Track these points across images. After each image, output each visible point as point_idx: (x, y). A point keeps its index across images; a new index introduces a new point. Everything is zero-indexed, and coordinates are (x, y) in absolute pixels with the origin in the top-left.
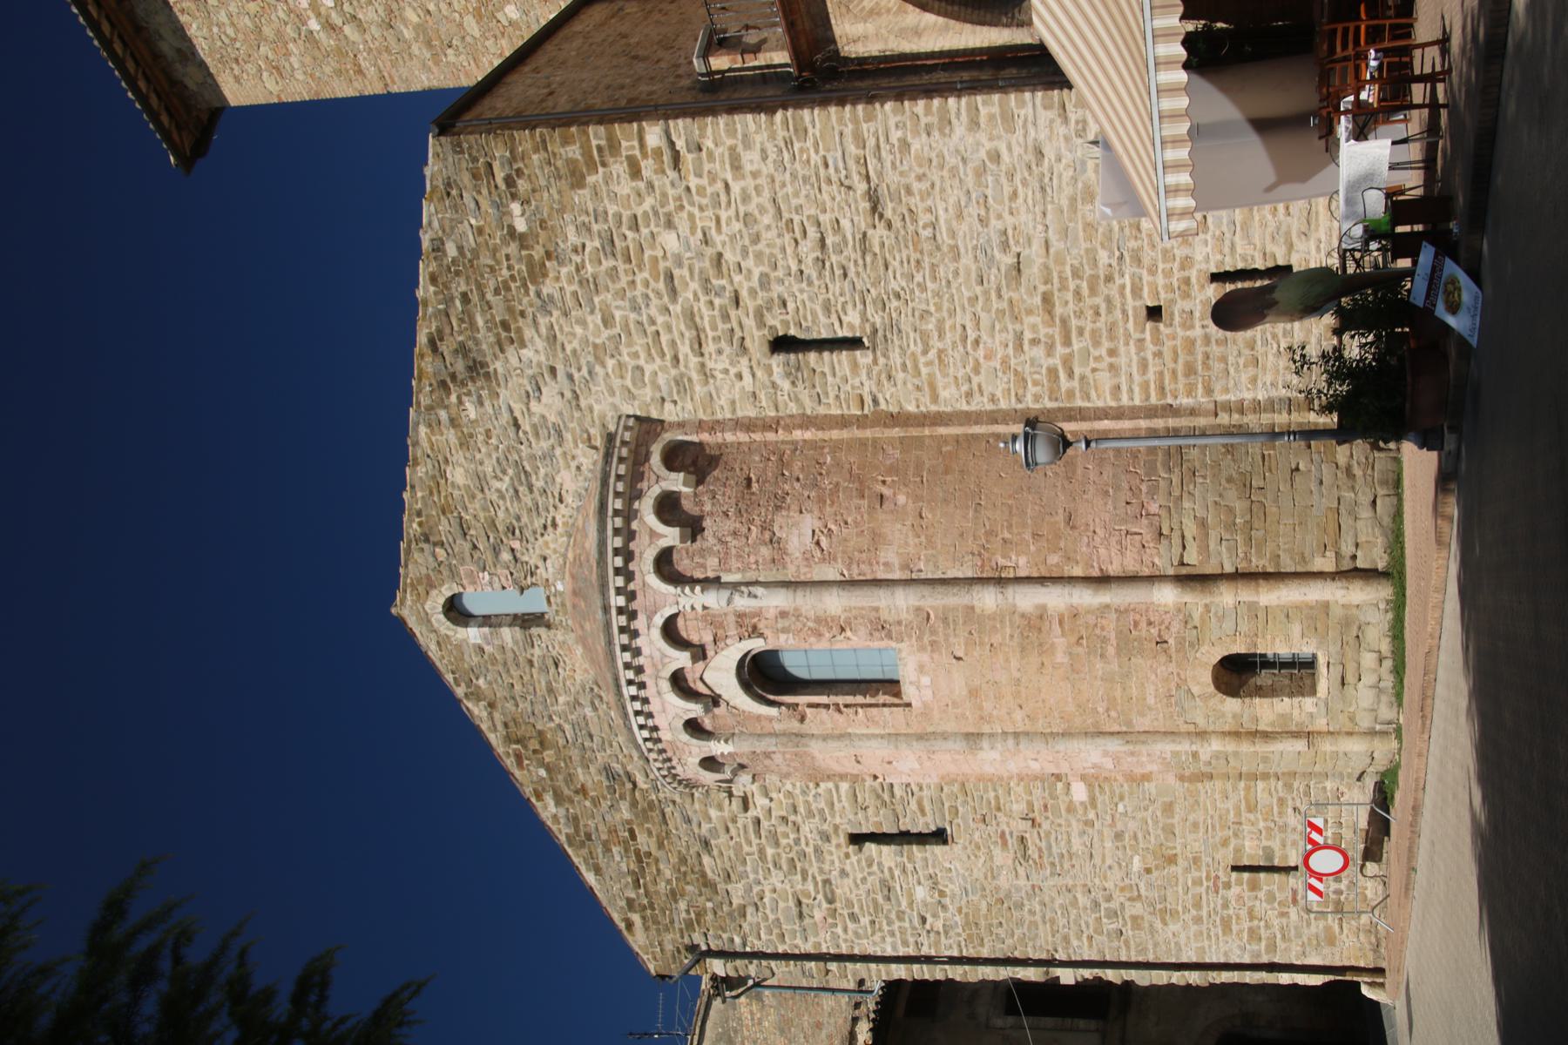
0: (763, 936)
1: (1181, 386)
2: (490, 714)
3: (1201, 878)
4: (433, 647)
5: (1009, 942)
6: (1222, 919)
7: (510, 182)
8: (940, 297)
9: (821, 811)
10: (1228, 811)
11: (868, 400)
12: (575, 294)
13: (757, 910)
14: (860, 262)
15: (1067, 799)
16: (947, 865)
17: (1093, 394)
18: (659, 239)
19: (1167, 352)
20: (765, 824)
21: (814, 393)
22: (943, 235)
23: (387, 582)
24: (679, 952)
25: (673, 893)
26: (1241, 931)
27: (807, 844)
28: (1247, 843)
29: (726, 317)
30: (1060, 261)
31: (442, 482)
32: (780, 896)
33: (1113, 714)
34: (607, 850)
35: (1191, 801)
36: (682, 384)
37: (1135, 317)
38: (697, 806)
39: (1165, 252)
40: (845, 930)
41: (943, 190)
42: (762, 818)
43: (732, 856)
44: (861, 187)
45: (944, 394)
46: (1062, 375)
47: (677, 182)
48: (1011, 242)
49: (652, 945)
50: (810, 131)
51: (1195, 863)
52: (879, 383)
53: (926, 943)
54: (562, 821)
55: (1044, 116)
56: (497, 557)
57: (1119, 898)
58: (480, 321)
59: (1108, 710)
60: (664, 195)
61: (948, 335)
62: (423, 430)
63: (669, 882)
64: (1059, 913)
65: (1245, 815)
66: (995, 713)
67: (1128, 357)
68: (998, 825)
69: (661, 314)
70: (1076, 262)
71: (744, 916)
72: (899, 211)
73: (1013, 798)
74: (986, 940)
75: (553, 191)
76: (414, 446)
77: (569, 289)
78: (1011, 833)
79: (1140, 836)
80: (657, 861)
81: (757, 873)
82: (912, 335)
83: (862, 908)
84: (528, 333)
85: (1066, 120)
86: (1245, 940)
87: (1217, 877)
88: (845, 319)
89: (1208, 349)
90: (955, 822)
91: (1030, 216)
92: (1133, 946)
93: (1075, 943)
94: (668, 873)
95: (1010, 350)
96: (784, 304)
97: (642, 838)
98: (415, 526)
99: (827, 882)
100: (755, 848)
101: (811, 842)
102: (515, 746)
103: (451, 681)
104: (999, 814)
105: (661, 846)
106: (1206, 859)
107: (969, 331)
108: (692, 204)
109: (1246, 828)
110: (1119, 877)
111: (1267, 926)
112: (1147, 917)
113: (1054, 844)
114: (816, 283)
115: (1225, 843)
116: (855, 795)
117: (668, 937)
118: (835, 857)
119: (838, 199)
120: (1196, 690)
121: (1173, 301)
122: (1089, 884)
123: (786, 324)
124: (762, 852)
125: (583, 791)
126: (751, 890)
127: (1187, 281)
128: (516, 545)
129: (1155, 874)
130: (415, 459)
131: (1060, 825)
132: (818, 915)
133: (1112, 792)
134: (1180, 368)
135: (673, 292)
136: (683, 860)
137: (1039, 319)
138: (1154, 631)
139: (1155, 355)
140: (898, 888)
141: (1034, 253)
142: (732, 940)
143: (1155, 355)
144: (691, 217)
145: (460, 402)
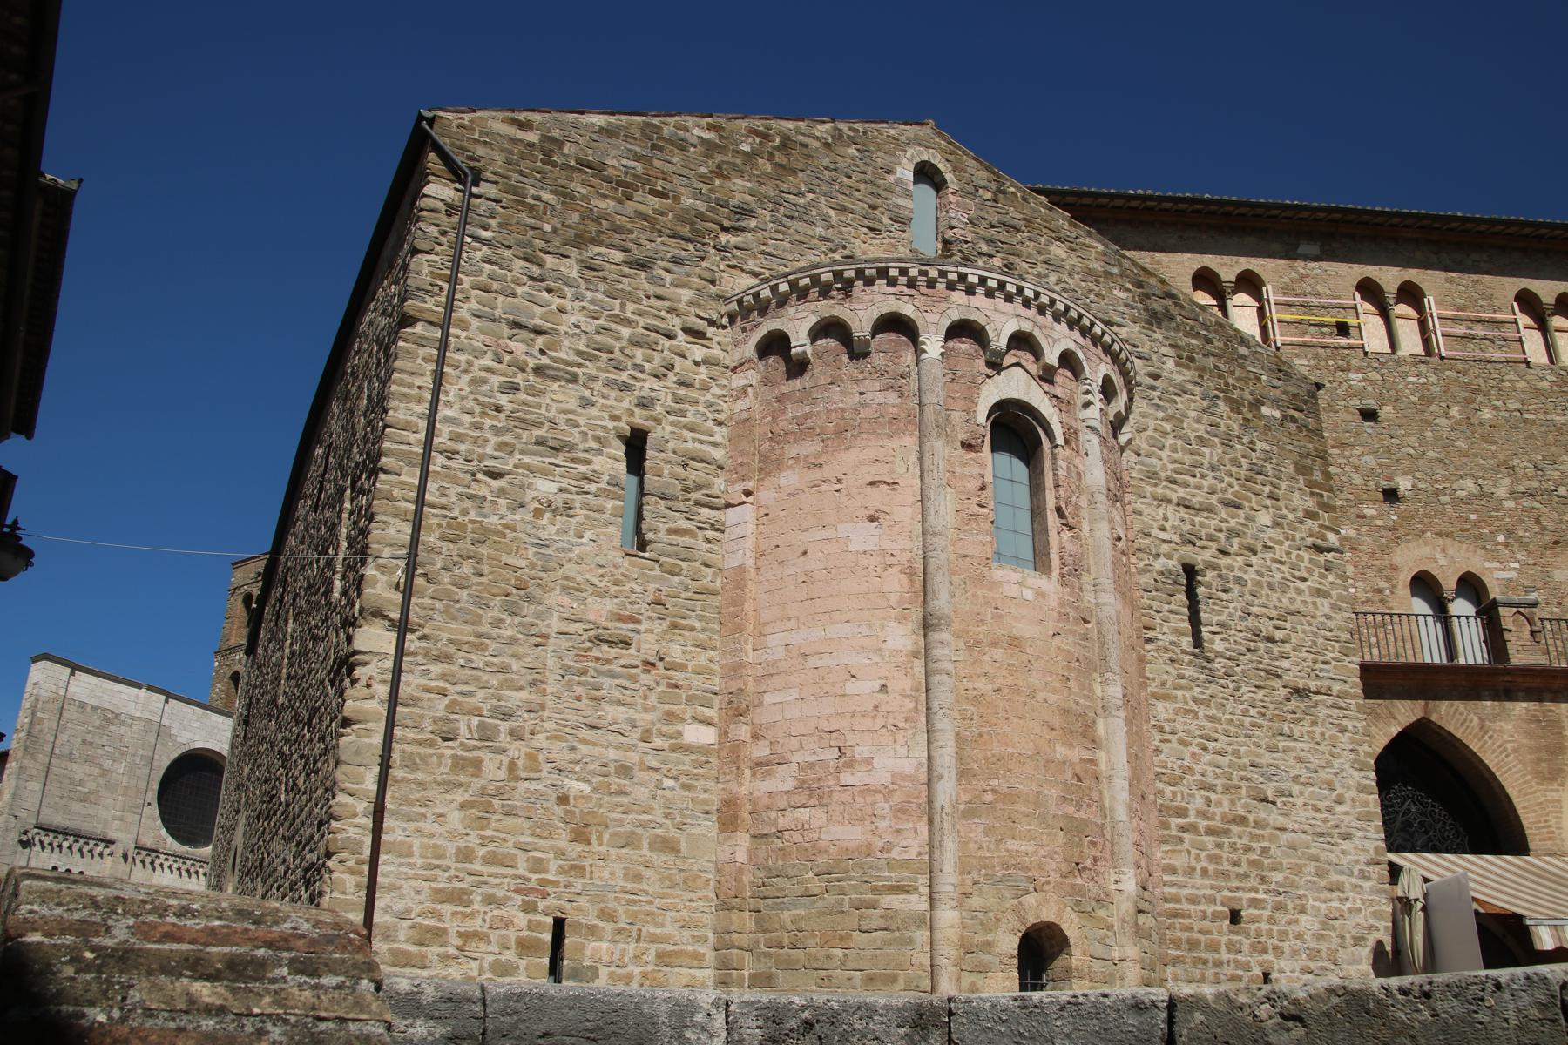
0: (487, 266)
1: (1178, 934)
2: (817, 138)
3: (546, 872)
4: (892, 132)
5: (446, 578)
6: (463, 891)
7: (1293, 420)
8: (1238, 726)
9: (682, 414)
10: (661, 926)
11: (1150, 634)
12: (1218, 425)
13: (532, 278)
14: (1261, 666)
15: (687, 716)
16: (588, 535)
17: (1166, 847)
18: (1264, 510)
19: (1207, 924)
20: (667, 343)
21: (1152, 588)
22: (1282, 743)
23: (960, 131)
24: (471, 159)
25: (573, 198)
26: (440, 917)
27: (634, 378)
28: (604, 945)
29: (1211, 538)
30: (1273, 838)
31: (1054, 235)
32: (551, 312)
33: (989, 797)
34: (637, 158)
35: (678, 878)
36: (1152, 477)
37: (1234, 898)
38: (696, 280)
39: (1285, 933)
40: (488, 370)
41: (1317, 751)
42: (674, 342)
43: (621, 286)
44: (1313, 685)
45: (1160, 706)
46: (1181, 821)
47: (1304, 543)
48: (1285, 799)
49: (487, 134)
50: (1347, 659)
51: (573, 867)
52: (1166, 650)
53: (450, 463)
54: (680, 133)
55: (1371, 845)
56: (984, 239)
57: (516, 750)
58: (1193, 341)
59: (995, 791)
60: (1295, 529)
61: (1210, 725)
62: (1101, 248)
63: (586, 198)
64: (495, 660)
65: (653, 948)
66: (987, 658)
67: (1201, 886)
68: (650, 618)
69: (1210, 487)
70: (1272, 852)
71: (525, 259)
72: (1298, 711)
73: (689, 648)
74: (451, 546)
75: (1290, 447)
76: (1089, 232)
77: (1222, 422)
78: (638, 632)
79: (623, 800)
80: (620, 202)
81: (592, 302)
82: (1208, 692)
83: (524, 404)
84: (1188, 374)
85: (1368, 863)
86: (419, 920)
87: (545, 896)
88: (1218, 637)
89: (1210, 965)
90: (657, 566)
91: (1303, 820)
92: (421, 750)
93: (436, 669)
94: (602, 204)
95: (1198, 777)
96: (1225, 591)
97: (655, 201)
98: (1012, 189)
99: (574, 379)
100: (629, 315)
101: (638, 385)
102: (778, 140)
103: (856, 126)
104: (665, 625)
105: (642, 216)
106: (579, 884)
107: (1214, 744)
108: (1290, 547)
109: (631, 948)
110: (553, 757)
111: (445, 958)
112: (477, 783)
113: (617, 682)
114: (1244, 624)
115: (607, 915)
116: (702, 461)
117: (499, 158)
118: (611, 402)
119: (1305, 664)
120: (1031, 900)
121: (1248, 936)
122: (546, 714)
123: (1209, 586)
124: (627, 322)
125: (719, 172)
126: (566, 284)
127: (1265, 951)
128: (997, 262)
129: (559, 810)
130: (1076, 226)
131: (645, 698)
132: (518, 347)
133: (697, 777)
134: (1195, 935)
135: (1227, 504)
136: (619, 230)
137: (1227, 810)
138: (1088, 863)
139: (1205, 912)
140: (552, 460)
141: (1274, 817)
142: (485, 227)
143: (1205, 912)
144: (1280, 543)
145: (1128, 290)
